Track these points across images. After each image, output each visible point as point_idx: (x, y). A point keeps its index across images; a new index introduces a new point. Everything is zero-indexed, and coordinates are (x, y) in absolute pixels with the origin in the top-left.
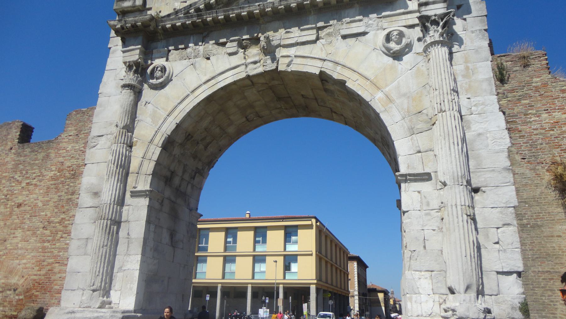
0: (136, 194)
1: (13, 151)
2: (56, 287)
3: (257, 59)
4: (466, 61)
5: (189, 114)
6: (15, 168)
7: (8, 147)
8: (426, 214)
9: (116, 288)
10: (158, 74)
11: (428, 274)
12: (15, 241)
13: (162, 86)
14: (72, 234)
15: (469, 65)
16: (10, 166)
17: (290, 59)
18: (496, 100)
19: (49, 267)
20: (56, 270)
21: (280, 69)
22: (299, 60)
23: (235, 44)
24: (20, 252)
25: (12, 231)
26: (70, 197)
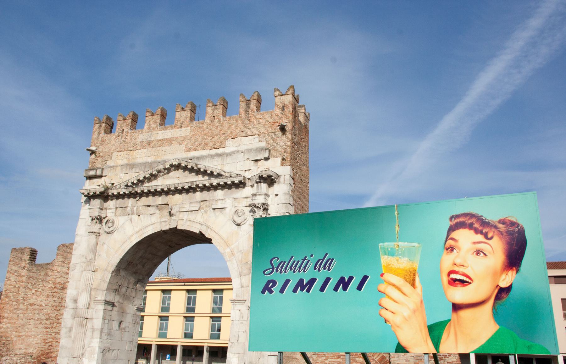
0: (97, 302)
1: (26, 268)
2: (54, 355)
3: (166, 220)
5: (128, 252)
6: (28, 281)
7: (23, 266)
8: (242, 323)
9: (87, 356)
10: (110, 225)
11: (237, 355)
12: (30, 327)
13: (111, 232)
14: (62, 324)
16: (24, 278)
19: (50, 344)
20: (54, 345)
21: (178, 228)
22: (188, 223)
23: (154, 208)
24: (33, 333)
25: (29, 321)
26: (60, 301)
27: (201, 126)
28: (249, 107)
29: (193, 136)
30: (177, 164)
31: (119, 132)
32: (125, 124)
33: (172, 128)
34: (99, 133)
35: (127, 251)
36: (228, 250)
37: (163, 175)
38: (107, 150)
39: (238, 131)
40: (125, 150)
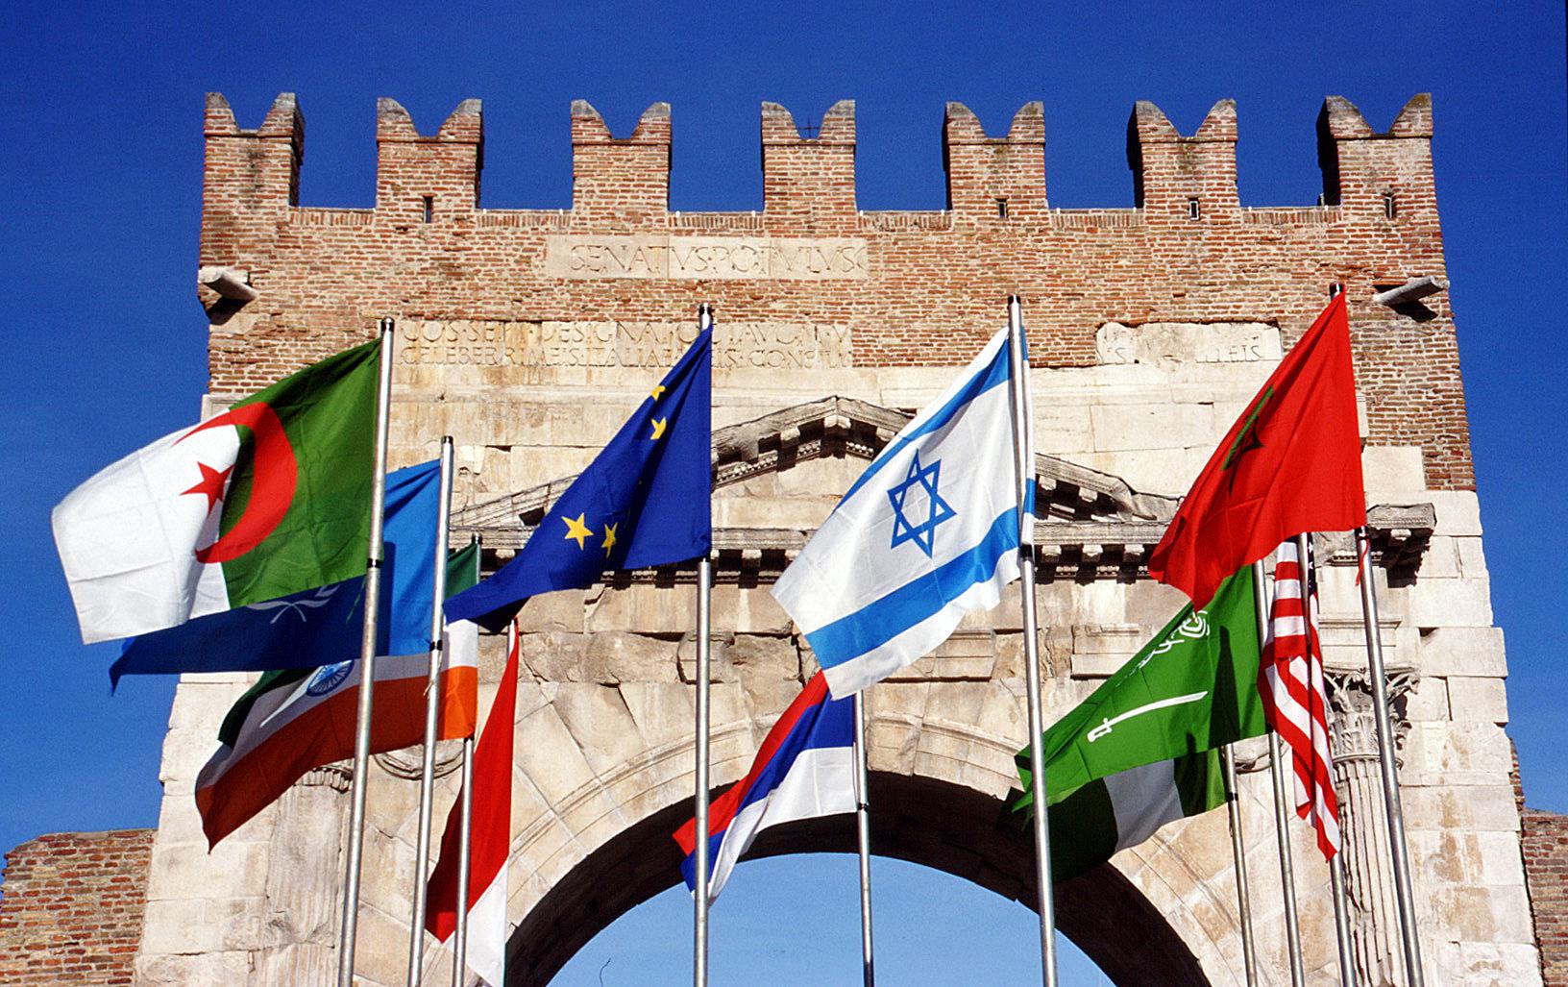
4: (1448, 822)
15: (1458, 834)
17: (911, 734)
18: (1535, 962)
27: (932, 239)
28: (1198, 176)
29: (895, 284)
30: (846, 424)
31: (407, 207)
32: (436, 166)
33: (754, 229)
34: (254, 194)
35: (554, 882)
36: (1196, 897)
37: (745, 476)
38: (331, 298)
39: (1155, 291)
40: (459, 316)
